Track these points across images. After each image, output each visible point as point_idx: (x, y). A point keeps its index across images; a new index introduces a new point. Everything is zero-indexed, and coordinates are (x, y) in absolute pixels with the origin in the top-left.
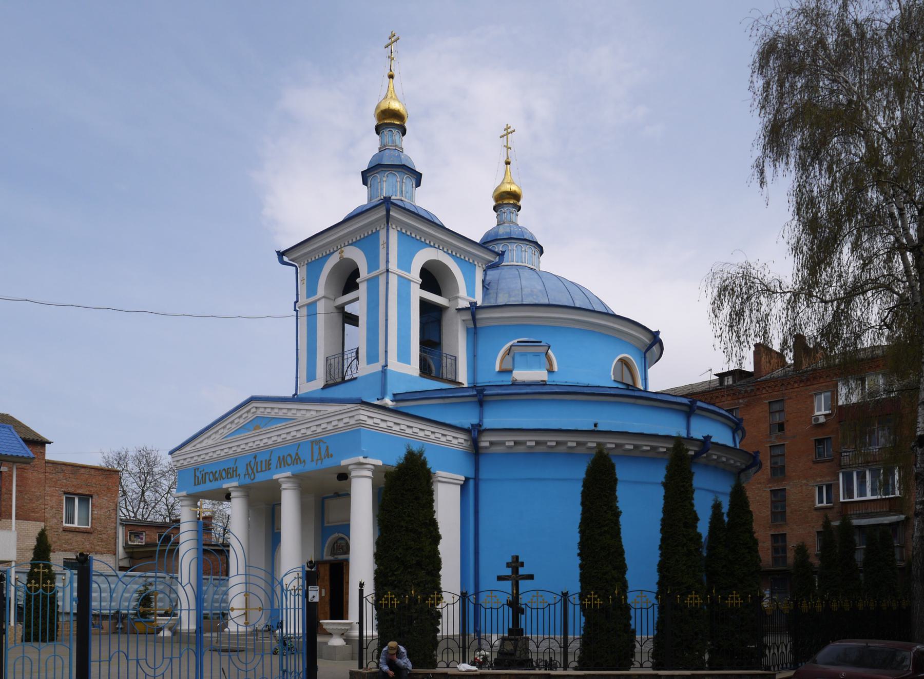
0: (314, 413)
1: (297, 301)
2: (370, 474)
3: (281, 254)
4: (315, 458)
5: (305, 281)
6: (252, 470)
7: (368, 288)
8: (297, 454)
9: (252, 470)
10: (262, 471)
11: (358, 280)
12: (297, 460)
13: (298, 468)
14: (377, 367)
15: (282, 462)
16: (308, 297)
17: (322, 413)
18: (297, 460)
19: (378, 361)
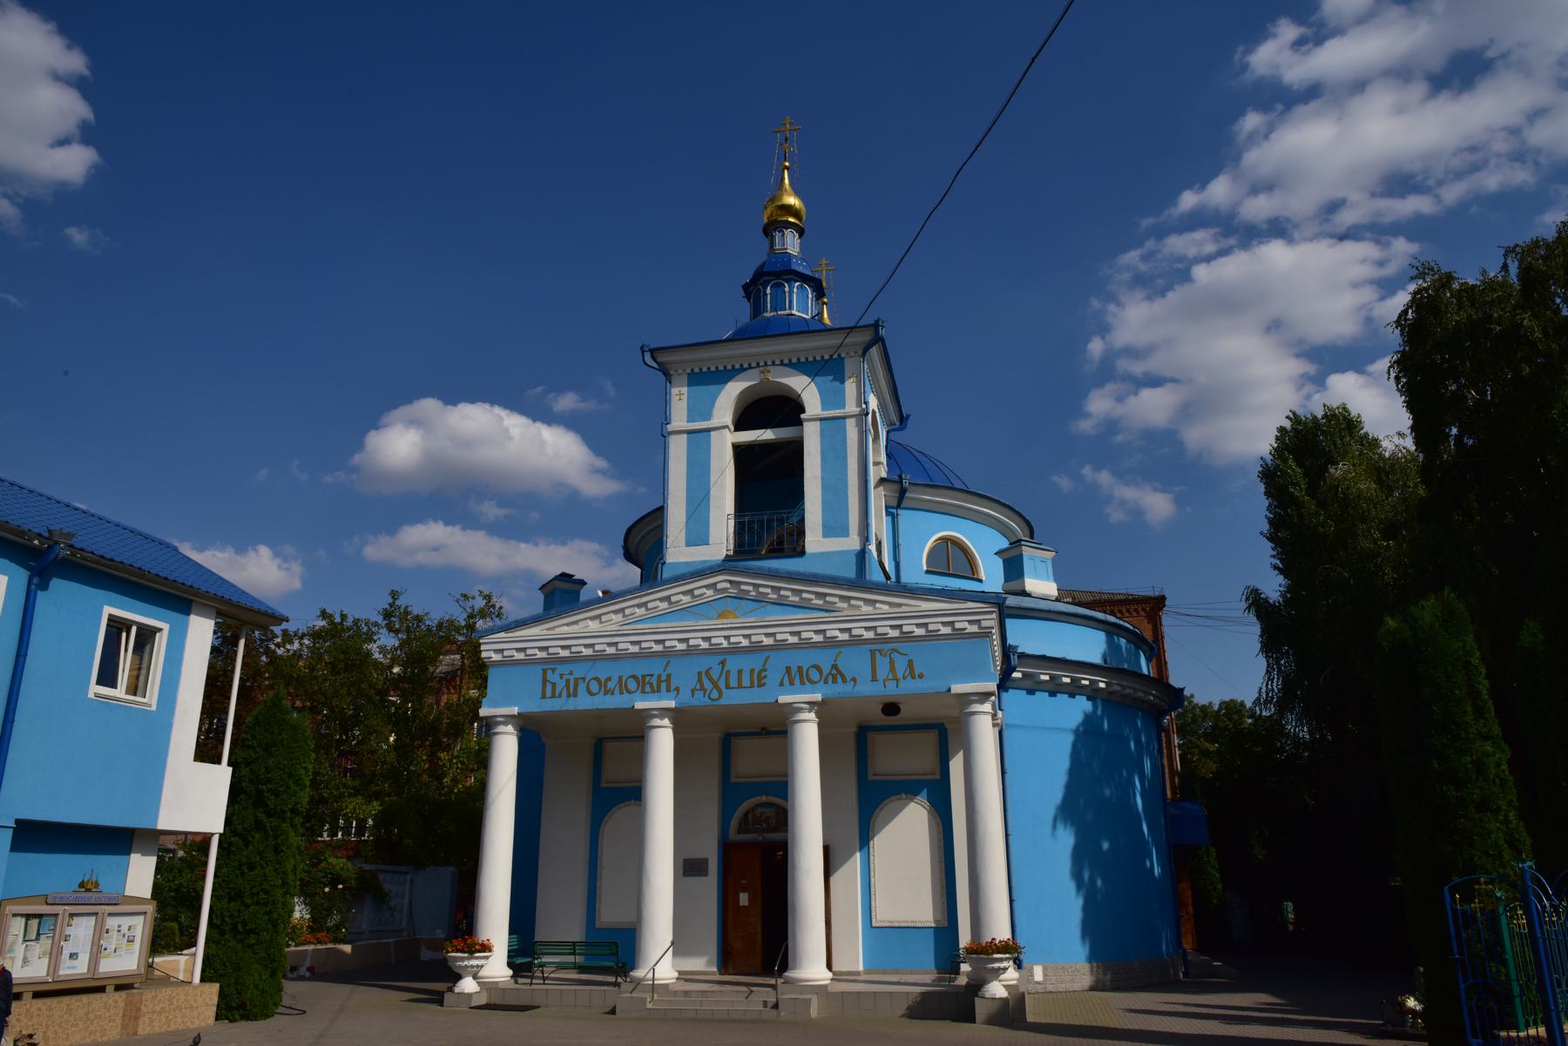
0: (886, 608)
6: (715, 684)
7: (822, 430)
8: (835, 667)
9: (715, 684)
10: (740, 686)
12: (836, 674)
14: (852, 543)
15: (797, 677)
16: (690, 420)
17: (904, 609)
18: (836, 674)
19: (847, 535)
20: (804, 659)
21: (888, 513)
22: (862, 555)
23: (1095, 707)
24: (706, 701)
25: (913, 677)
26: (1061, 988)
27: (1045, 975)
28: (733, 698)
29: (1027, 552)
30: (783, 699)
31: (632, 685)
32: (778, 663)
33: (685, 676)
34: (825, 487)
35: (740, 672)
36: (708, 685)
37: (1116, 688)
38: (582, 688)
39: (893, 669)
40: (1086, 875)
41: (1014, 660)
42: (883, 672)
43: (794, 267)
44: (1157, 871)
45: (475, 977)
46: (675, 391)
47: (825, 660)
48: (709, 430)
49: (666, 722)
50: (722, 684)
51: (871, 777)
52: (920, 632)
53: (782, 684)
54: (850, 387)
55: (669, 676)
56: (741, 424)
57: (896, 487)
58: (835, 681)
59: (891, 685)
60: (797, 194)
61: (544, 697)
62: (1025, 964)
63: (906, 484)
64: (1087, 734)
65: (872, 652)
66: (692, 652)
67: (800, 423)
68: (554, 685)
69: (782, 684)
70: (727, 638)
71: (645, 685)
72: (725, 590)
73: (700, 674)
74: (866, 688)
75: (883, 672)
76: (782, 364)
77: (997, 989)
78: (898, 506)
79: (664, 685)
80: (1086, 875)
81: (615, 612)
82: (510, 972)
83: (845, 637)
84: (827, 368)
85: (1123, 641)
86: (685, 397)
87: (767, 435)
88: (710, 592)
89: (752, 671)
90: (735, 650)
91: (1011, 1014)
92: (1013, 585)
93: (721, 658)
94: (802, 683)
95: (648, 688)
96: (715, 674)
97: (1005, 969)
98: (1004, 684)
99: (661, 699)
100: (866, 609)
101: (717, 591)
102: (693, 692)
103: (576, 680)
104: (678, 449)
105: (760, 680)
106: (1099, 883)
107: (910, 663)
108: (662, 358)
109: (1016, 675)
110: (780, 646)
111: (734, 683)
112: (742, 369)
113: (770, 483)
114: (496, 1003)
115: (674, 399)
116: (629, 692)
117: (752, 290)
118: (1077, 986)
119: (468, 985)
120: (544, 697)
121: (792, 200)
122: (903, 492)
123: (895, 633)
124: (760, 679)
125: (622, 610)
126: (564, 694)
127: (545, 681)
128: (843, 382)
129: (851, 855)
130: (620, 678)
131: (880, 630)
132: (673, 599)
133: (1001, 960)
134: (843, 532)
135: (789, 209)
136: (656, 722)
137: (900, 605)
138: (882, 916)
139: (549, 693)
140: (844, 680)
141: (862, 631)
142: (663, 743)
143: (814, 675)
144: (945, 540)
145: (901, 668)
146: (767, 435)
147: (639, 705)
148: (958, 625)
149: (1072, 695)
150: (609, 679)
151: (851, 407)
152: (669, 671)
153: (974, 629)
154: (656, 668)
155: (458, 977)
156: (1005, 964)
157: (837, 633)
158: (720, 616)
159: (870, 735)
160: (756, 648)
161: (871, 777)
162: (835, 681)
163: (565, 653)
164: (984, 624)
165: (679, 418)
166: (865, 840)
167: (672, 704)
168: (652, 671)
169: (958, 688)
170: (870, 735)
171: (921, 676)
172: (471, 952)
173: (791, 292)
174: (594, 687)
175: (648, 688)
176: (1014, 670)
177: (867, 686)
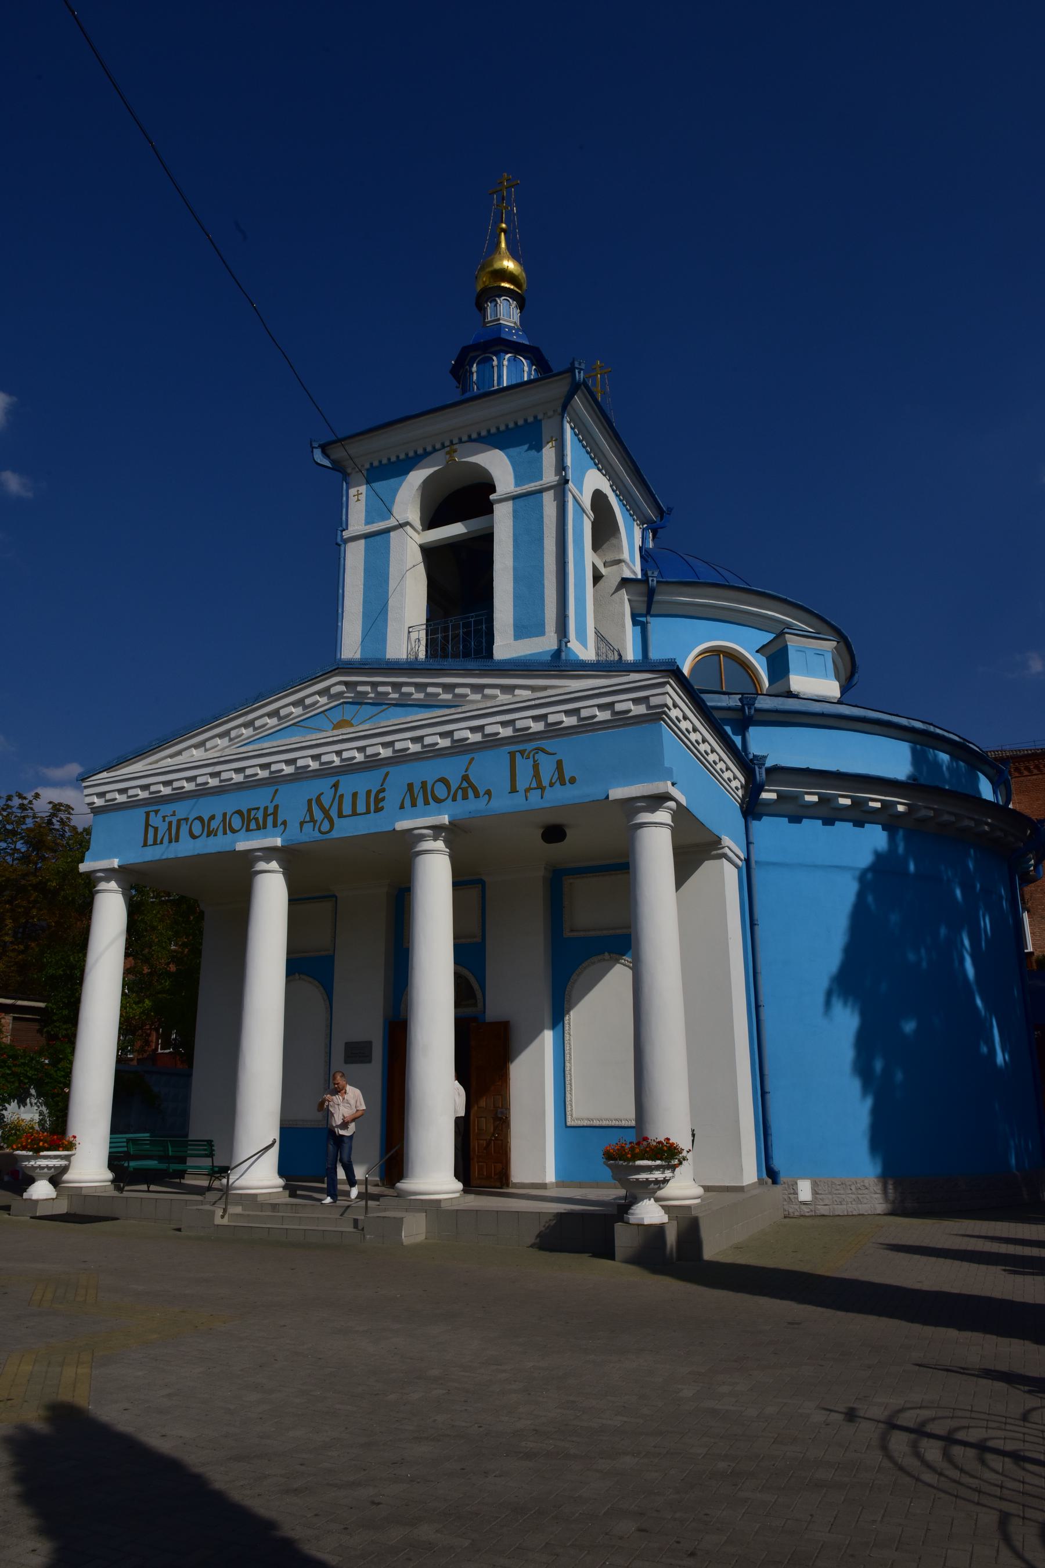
0: (526, 694)
4: (522, 784)
7: (515, 511)
8: (465, 778)
10: (355, 813)
11: (492, 497)
12: (468, 788)
15: (420, 796)
16: (367, 523)
18: (468, 788)
19: (542, 633)
20: (429, 771)
21: (635, 623)
23: (892, 839)
24: (316, 835)
25: (563, 783)
26: (840, 1210)
27: (815, 1193)
28: (347, 828)
29: (793, 642)
30: (402, 825)
31: (237, 822)
32: (400, 778)
33: (293, 804)
34: (518, 578)
35: (355, 795)
36: (318, 815)
37: (924, 813)
39: (537, 775)
40: (878, 1065)
41: (761, 775)
42: (524, 779)
43: (503, 336)
44: (1000, 1058)
45: (55, 1180)
46: (352, 491)
47: (453, 770)
48: (387, 531)
49: (274, 865)
50: (334, 813)
51: (567, 934)
52: (570, 721)
53: (402, 807)
54: (549, 453)
55: (276, 807)
56: (431, 522)
57: (643, 588)
58: (465, 797)
59: (534, 796)
60: (514, 256)
61: (145, 845)
62: (783, 1178)
63: (653, 582)
64: (878, 877)
65: (512, 755)
66: (302, 775)
68: (156, 829)
69: (402, 807)
70: (339, 753)
71: (251, 821)
72: (340, 694)
73: (310, 801)
74: (503, 803)
75: (524, 779)
76: (470, 440)
77: (649, 1212)
78: (648, 613)
79: (270, 819)
80: (878, 1065)
81: (220, 736)
82: (109, 1175)
83: (477, 737)
84: (522, 436)
85: (944, 757)
86: (363, 497)
87: (456, 529)
88: (323, 700)
89: (369, 793)
90: (350, 768)
91: (677, 1253)
92: (779, 687)
93: (332, 780)
94: (426, 803)
95: (253, 825)
96: (326, 802)
97: (666, 1181)
98: (751, 808)
99: (266, 837)
100: (503, 698)
101: (332, 697)
102: (302, 824)
103: (179, 821)
104: (354, 557)
105: (376, 802)
106: (899, 1076)
107: (559, 764)
108: (338, 453)
109: (765, 795)
110: (401, 758)
111: (347, 809)
112: (426, 454)
113: (460, 585)
114: (81, 1213)
115: (352, 500)
116: (233, 831)
117: (459, 372)
118: (864, 1208)
119: (41, 1190)
120: (145, 845)
121: (509, 265)
122: (651, 594)
123: (538, 727)
124: (378, 801)
125: (226, 733)
126: (166, 840)
127: (147, 825)
128: (539, 448)
129: (537, 1032)
130: (225, 815)
131: (519, 724)
132: (283, 712)
133: (650, 1169)
134: (539, 630)
135: (504, 274)
136: (262, 866)
137: (545, 688)
138: (580, 1112)
139: (150, 841)
140: (477, 796)
141: (499, 729)
142: (272, 896)
143: (441, 791)
144: (716, 651)
145: (547, 772)
146: (456, 529)
147: (242, 846)
148: (618, 707)
149: (859, 824)
150: (213, 817)
151: (549, 476)
152: (275, 803)
153: (641, 709)
154: (260, 799)
155: (31, 1181)
156: (658, 1175)
157: (467, 734)
158: (337, 726)
160: (373, 763)
161: (567, 934)
162: (465, 797)
163: (166, 791)
164: (654, 701)
165: (357, 521)
166: (558, 1019)
167: (278, 842)
168: (255, 800)
169: (618, 793)
171: (573, 780)
172: (37, 1150)
173: (500, 366)
174: (197, 828)
175: (253, 825)
176: (761, 789)
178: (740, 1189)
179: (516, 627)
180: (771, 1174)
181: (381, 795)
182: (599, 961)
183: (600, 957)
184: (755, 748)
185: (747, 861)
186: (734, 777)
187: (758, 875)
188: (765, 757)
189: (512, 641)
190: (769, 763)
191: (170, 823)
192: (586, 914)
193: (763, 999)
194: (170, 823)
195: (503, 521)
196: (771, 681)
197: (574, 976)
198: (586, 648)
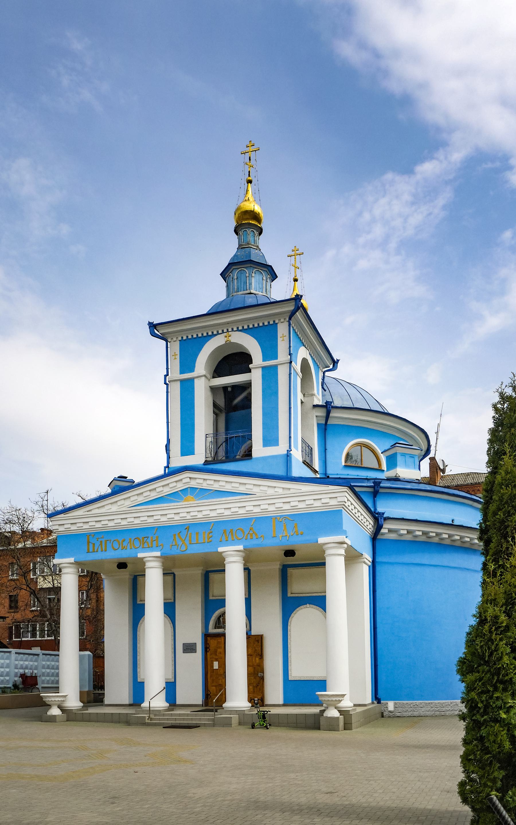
1: (167, 375)
2: (343, 552)
3: (153, 326)
5: (178, 357)
13: (253, 543)
14: (281, 449)
16: (182, 372)
22: (288, 456)
38: (109, 545)
41: (381, 521)
61: (88, 552)
67: (249, 371)
126: (100, 550)
139: (91, 550)
159: (290, 571)
170: (290, 571)
177: (275, 541)
178: (365, 705)
179: (264, 440)
180: (377, 698)
181: (210, 535)
182: (304, 608)
183: (305, 606)
184: (380, 510)
185: (374, 562)
186: (369, 523)
187: (378, 568)
188: (383, 514)
189: (262, 447)
190: (385, 516)
191: (101, 542)
192: (299, 586)
193: (378, 625)
194: (101, 542)
195: (256, 378)
196: (388, 469)
197: (292, 615)
198: (297, 449)
